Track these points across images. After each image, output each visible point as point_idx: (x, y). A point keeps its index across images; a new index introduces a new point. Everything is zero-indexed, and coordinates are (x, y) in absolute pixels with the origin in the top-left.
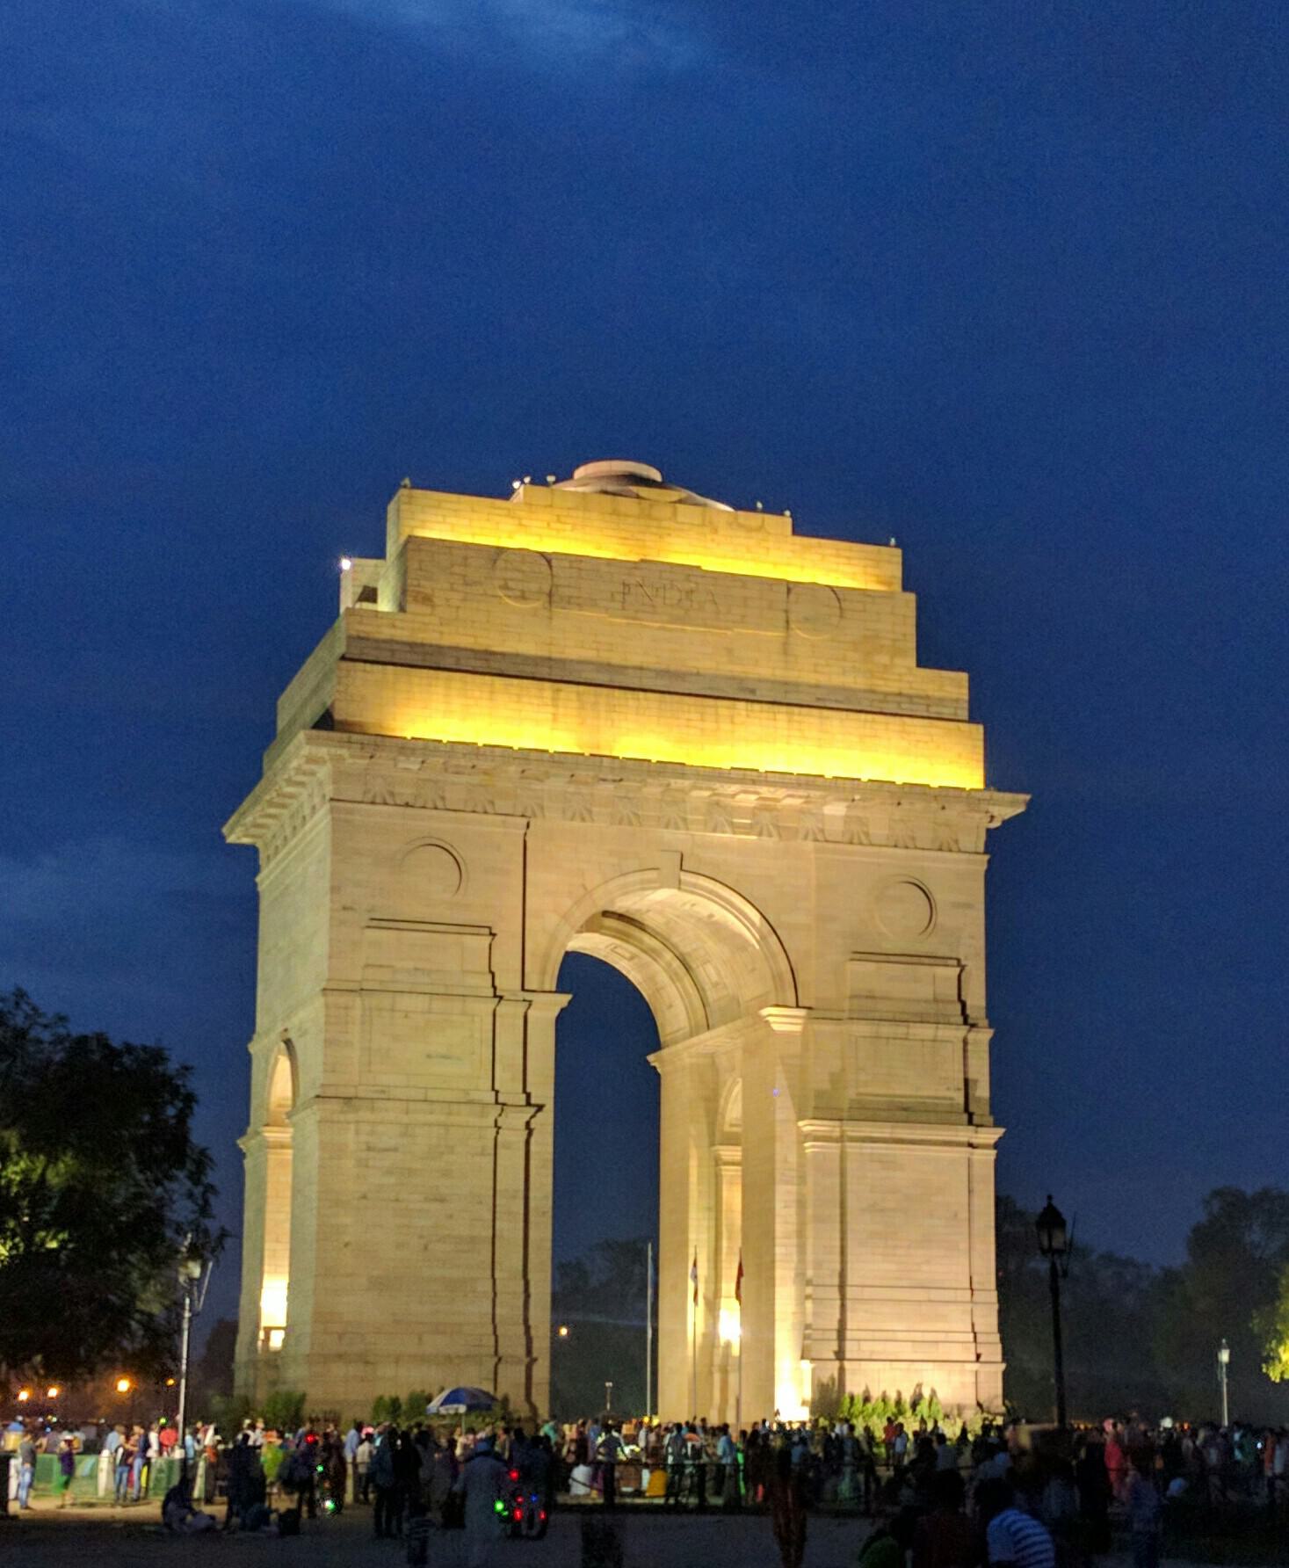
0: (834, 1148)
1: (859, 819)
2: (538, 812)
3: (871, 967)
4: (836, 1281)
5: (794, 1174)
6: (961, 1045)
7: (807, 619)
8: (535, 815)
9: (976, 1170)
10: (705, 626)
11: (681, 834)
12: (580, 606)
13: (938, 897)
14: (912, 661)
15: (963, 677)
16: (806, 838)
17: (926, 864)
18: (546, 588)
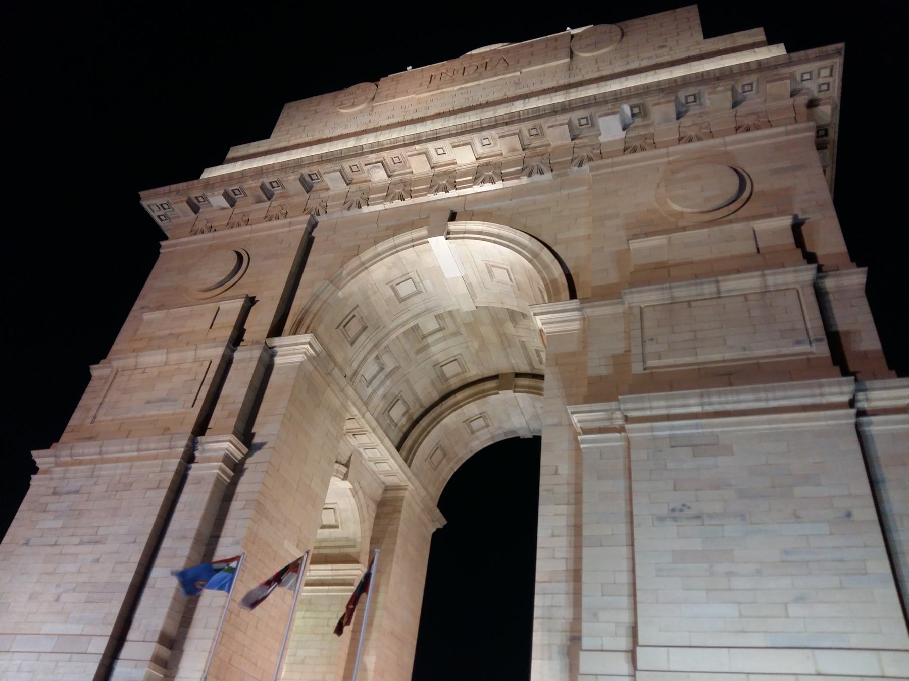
1: (645, 137)
2: (321, 211)
4: (624, 643)
6: (810, 291)
7: (588, 46)
8: (318, 214)
9: (880, 449)
10: (496, 75)
11: (453, 193)
12: (394, 97)
13: (751, 169)
16: (580, 165)
17: (729, 148)
18: (372, 96)
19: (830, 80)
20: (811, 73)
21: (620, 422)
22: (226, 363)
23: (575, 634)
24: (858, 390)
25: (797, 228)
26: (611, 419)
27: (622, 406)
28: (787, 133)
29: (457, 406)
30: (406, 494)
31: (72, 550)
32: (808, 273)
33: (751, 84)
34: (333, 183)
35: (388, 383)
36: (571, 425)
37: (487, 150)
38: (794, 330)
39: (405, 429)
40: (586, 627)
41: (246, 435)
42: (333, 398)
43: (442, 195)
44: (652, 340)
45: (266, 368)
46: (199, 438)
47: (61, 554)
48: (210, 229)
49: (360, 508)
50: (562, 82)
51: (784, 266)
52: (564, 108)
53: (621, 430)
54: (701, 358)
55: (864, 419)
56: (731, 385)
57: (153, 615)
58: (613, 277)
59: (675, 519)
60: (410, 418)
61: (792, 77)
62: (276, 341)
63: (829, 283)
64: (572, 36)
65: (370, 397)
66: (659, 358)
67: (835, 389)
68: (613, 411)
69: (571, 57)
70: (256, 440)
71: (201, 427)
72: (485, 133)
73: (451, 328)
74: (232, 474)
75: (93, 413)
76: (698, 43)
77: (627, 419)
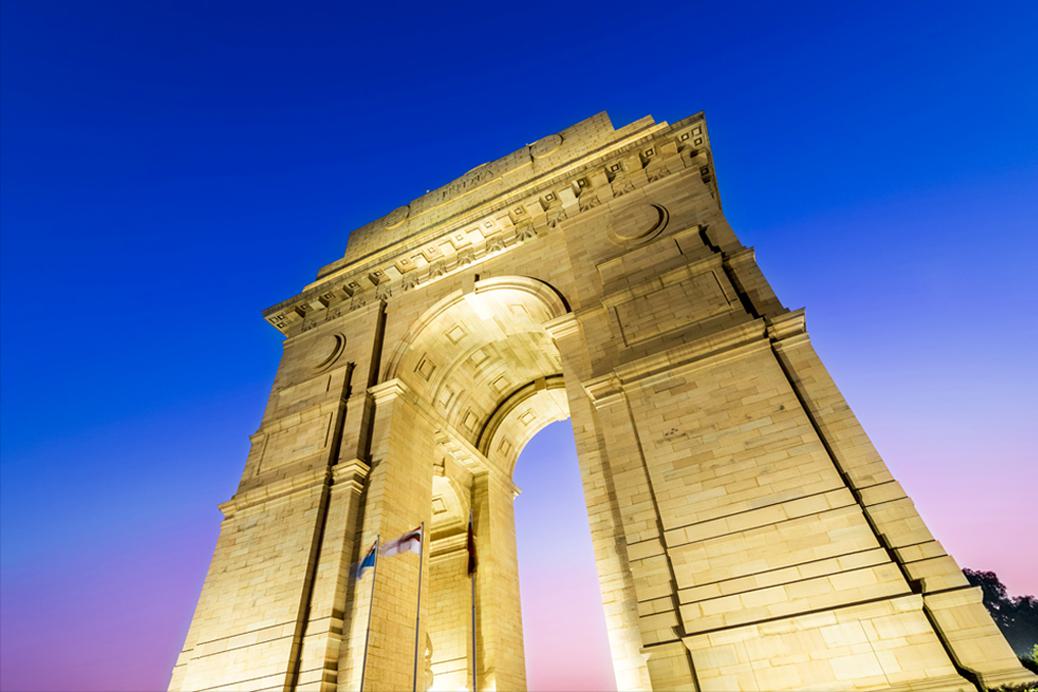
0: (618, 399)
1: (592, 199)
2: (388, 295)
3: (618, 261)
4: (655, 533)
5: (595, 439)
8: (386, 298)
9: (793, 360)
11: (474, 263)
14: (612, 129)
15: (649, 116)
16: (554, 226)
17: (647, 194)
18: (406, 214)
19: (701, 136)
20: (687, 134)
21: (619, 385)
22: (343, 411)
23: (621, 536)
24: (767, 326)
25: (702, 232)
26: (611, 385)
27: (617, 374)
28: (682, 175)
29: (511, 408)
30: (489, 477)
31: (258, 567)
32: (717, 260)
33: (651, 150)
34: (392, 275)
35: (459, 403)
36: (587, 396)
37: (491, 230)
38: (717, 297)
39: (478, 433)
40: (626, 529)
41: (366, 458)
42: (422, 421)
43: (466, 266)
44: (626, 326)
45: (371, 408)
46: (334, 467)
47: (251, 572)
48: (315, 325)
49: (459, 494)
50: (530, 177)
51: (700, 259)
52: (535, 192)
53: (621, 390)
54: (662, 331)
55: (775, 344)
56: (684, 342)
57: (326, 599)
58: (593, 292)
59: (669, 440)
60: (480, 424)
61: (676, 139)
62: (374, 389)
63: (732, 262)
64: (530, 148)
65: (449, 415)
66: (634, 337)
67: (752, 329)
68: (612, 379)
69: (532, 158)
70: (374, 460)
71: (334, 459)
72: (486, 219)
73: (495, 355)
74: (362, 486)
75: (256, 468)
76: (612, 134)
77: (622, 382)
